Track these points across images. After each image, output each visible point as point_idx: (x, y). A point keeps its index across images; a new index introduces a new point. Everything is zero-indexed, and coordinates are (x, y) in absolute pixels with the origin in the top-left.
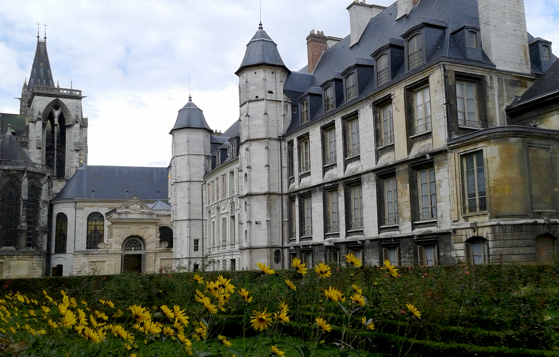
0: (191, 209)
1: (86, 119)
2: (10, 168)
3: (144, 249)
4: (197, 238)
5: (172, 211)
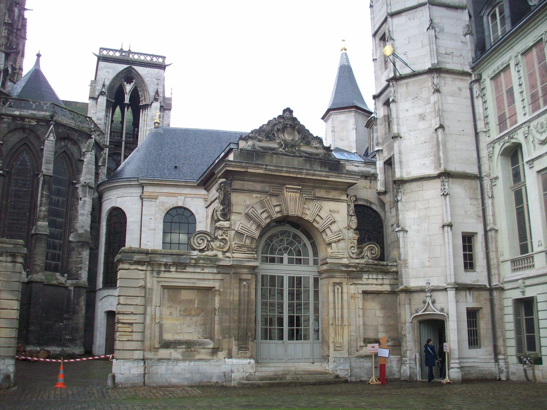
0: (449, 146)
1: (170, 99)
2: (25, 113)
3: (316, 262)
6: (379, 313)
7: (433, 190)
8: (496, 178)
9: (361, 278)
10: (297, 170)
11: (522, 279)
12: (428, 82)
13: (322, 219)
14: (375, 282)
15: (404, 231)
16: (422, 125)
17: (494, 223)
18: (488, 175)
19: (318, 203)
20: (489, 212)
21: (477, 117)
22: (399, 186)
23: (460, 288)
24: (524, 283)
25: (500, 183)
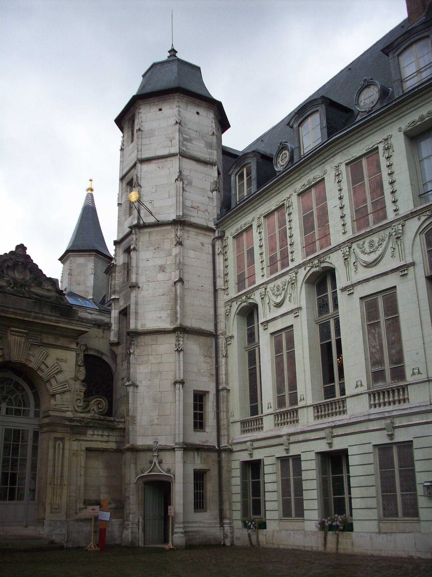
3: (37, 414)
4: (201, 388)
5: (115, 313)
6: (102, 473)
7: (167, 345)
8: (232, 337)
9: (85, 434)
10: (24, 313)
11: (250, 441)
12: (171, 233)
13: (48, 367)
14: (100, 438)
15: (135, 386)
16: (161, 276)
17: (227, 383)
18: (224, 334)
19: (44, 350)
20: (222, 371)
21: (218, 274)
22: (133, 338)
23: (189, 448)
24: (252, 445)
25: (235, 342)
